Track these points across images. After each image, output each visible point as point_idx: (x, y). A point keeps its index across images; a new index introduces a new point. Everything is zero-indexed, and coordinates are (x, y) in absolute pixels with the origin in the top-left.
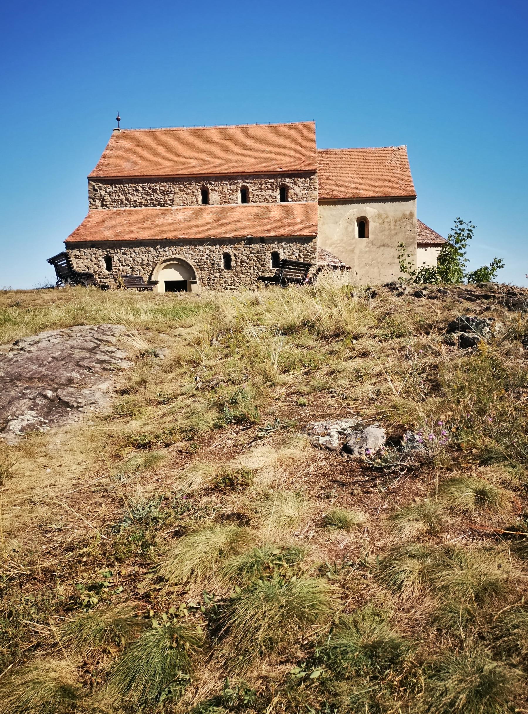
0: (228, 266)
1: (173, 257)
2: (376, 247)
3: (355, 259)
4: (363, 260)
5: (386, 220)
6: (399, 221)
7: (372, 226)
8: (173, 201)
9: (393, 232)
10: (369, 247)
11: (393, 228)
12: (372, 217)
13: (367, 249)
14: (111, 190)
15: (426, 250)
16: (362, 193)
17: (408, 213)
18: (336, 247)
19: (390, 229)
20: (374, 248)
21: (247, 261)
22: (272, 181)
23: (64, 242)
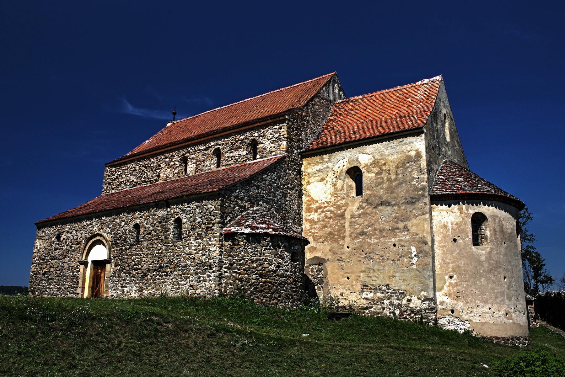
2: (372, 207)
4: (357, 227)
5: (384, 168)
6: (401, 167)
10: (363, 208)
11: (393, 177)
12: (366, 165)
13: (361, 211)
17: (413, 153)
18: (323, 212)
19: (389, 180)
22: (242, 137)
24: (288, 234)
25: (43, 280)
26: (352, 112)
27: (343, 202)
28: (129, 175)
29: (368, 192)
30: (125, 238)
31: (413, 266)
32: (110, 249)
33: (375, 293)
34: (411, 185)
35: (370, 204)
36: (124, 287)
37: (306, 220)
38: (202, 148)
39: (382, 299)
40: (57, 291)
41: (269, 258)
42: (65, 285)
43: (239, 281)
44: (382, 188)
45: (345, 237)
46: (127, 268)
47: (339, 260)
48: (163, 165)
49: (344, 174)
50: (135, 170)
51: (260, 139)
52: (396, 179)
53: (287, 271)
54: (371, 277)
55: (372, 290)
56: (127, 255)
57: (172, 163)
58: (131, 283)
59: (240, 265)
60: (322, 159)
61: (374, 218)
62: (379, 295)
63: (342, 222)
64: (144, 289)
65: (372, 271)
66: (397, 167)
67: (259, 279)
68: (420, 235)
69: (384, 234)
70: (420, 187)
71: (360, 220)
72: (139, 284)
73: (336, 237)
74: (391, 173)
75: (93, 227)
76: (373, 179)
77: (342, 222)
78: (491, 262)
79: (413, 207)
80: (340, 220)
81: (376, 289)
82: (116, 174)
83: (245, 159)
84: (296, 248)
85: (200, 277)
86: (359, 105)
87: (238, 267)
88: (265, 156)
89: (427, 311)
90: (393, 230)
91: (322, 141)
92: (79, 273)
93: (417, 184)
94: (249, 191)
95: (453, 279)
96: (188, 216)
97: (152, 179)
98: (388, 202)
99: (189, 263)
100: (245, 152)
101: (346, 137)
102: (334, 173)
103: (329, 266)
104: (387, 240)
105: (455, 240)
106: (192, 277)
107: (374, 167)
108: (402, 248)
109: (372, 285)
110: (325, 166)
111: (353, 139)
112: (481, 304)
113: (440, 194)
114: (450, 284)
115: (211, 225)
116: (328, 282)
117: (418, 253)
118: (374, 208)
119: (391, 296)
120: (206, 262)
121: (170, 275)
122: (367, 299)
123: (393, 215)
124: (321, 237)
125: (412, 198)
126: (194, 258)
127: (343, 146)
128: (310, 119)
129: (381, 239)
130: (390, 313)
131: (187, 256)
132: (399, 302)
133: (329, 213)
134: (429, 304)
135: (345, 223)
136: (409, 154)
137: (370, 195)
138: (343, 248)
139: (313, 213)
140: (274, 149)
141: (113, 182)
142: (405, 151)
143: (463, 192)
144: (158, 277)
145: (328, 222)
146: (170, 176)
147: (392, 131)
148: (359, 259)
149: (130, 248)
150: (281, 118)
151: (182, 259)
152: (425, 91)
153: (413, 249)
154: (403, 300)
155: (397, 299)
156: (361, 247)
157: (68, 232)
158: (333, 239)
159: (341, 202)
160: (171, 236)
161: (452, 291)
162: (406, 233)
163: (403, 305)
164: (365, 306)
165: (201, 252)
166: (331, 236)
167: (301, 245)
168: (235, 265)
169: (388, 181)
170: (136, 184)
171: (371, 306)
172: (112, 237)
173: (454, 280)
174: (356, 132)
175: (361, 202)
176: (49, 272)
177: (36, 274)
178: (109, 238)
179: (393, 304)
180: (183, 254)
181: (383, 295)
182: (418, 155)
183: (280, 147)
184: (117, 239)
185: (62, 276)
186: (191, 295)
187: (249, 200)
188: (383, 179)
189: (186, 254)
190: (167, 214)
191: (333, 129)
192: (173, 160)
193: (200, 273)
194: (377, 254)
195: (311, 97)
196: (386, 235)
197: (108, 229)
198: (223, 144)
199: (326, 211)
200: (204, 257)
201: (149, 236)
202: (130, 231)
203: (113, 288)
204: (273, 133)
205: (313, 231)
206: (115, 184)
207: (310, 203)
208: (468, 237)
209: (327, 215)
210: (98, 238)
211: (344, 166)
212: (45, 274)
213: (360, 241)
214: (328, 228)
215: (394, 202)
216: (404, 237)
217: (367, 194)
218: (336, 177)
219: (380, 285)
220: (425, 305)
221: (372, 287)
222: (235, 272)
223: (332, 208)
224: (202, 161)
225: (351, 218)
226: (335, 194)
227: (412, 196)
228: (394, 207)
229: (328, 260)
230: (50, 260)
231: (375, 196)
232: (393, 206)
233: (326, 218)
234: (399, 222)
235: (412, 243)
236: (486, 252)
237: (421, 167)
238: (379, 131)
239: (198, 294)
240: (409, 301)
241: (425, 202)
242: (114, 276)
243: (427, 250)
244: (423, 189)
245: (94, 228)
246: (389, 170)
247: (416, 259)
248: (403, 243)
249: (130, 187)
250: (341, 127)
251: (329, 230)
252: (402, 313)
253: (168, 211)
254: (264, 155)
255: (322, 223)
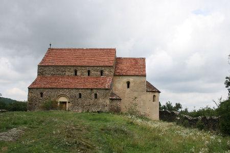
7: (131, 85)
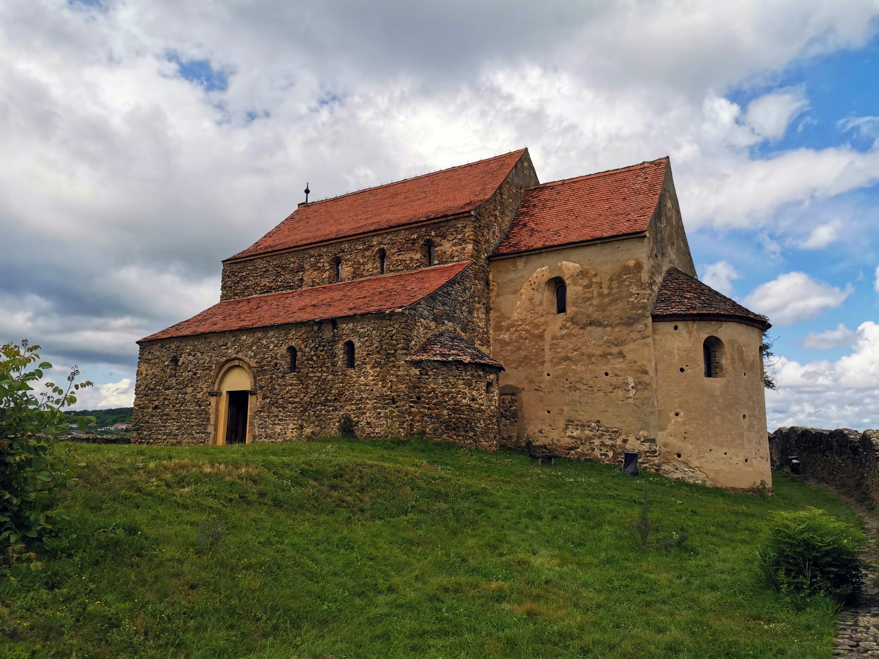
0: (293, 367)
1: (233, 356)
2: (579, 327)
3: (545, 350)
4: (559, 350)
6: (616, 280)
7: (571, 291)
8: (302, 280)
9: (607, 300)
10: (567, 328)
11: (606, 291)
12: (572, 276)
13: (565, 332)
14: (243, 274)
15: (676, 328)
16: (561, 240)
17: (631, 263)
18: (516, 331)
19: (601, 295)
20: (575, 331)
21: (315, 358)
23: (138, 343)
24: (483, 362)
25: (153, 416)
26: (549, 204)
27: (542, 320)
28: (259, 277)
29: (574, 309)
30: (276, 364)
31: (630, 400)
32: (255, 378)
33: (582, 431)
34: (628, 302)
35: (577, 323)
36: (276, 424)
37: (495, 340)
38: (361, 247)
39: (591, 438)
40: (177, 430)
41: (462, 390)
42: (188, 422)
43: (428, 418)
44: (591, 305)
45: (544, 362)
46: (280, 401)
47: (538, 390)
48: (307, 267)
49: (543, 285)
50: (268, 270)
51: (438, 240)
52: (609, 294)
53: (482, 405)
54: (576, 411)
55: (578, 427)
56: (279, 385)
57: (319, 265)
58: (286, 420)
59: (429, 398)
60: (515, 266)
61: (581, 341)
62: (587, 432)
63: (540, 344)
64: (305, 427)
65: (578, 404)
66: (611, 280)
67: (451, 415)
68: (639, 363)
69: (593, 360)
70: (639, 306)
71: (563, 343)
72: (297, 421)
73: (533, 362)
74: (603, 286)
75: (228, 348)
76: (580, 293)
77: (540, 344)
78: (727, 397)
79: (630, 329)
80: (537, 341)
81: (583, 426)
82: (240, 275)
83: (419, 264)
84: (492, 376)
85: (380, 413)
86: (557, 194)
87: (427, 401)
88: (446, 262)
89: (648, 454)
90: (604, 356)
91: (513, 242)
92: (209, 407)
93: (636, 301)
94: (434, 309)
95: (680, 416)
96: (362, 339)
97: (292, 284)
98: (600, 323)
99: (365, 396)
100: (418, 256)
101: (544, 239)
102: (531, 285)
103: (524, 396)
104: (597, 368)
105: (682, 370)
106: (370, 413)
107: (581, 279)
108: (616, 378)
109: (579, 420)
110: (519, 275)
111: (556, 243)
112: (714, 448)
113: (665, 314)
114: (676, 422)
115: (393, 351)
116: (523, 417)
117: (636, 385)
118: (581, 328)
119: (602, 434)
120: (387, 396)
121: (340, 410)
122: (573, 438)
123: (605, 338)
124: (514, 361)
125: (629, 318)
126: (372, 390)
127: (543, 251)
128: (498, 214)
129: (590, 366)
130: (601, 455)
131: (363, 388)
132: (612, 442)
133: (524, 332)
134: (650, 446)
135: (544, 346)
136: (626, 264)
137: (576, 313)
138: (542, 376)
139: (504, 332)
140: (457, 253)
141: (236, 285)
142: (621, 259)
143: (693, 312)
144: (323, 412)
145: (523, 343)
146: (318, 281)
147: (605, 235)
148: (563, 389)
149: (282, 377)
150: (467, 215)
151: (356, 392)
152: (647, 178)
153: (631, 381)
154: (618, 439)
155: (610, 439)
156: (565, 374)
157: (189, 354)
158: (530, 365)
159: (539, 319)
160: (339, 363)
161: (678, 430)
162: (621, 360)
163: (618, 447)
164: (570, 446)
165: (380, 383)
166: (528, 361)
167: (496, 373)
168: (423, 399)
169: (598, 296)
170: (270, 289)
171: (577, 446)
172: (256, 362)
173: (681, 418)
174: (557, 233)
175: (564, 320)
176: (163, 405)
177: (143, 408)
178: (253, 363)
179: (606, 446)
180: (356, 385)
181: (592, 433)
182: (639, 266)
183: (465, 251)
184: (264, 365)
185: (183, 410)
186: (368, 434)
187: (435, 320)
188: (593, 294)
189: (361, 385)
190: (334, 336)
191: (525, 225)
192: (322, 261)
193: (379, 408)
194: (584, 384)
195: (499, 184)
196: (596, 361)
197: (250, 353)
198: (389, 244)
199: (520, 330)
200: (386, 388)
201: (310, 362)
202: (282, 356)
203: (261, 426)
204: (455, 233)
205: (504, 354)
206: (238, 288)
207: (500, 320)
208: (698, 366)
209: (522, 335)
210: (237, 363)
211: (543, 276)
212: (156, 407)
213: (564, 368)
214: (523, 351)
215: (606, 322)
216: (618, 364)
217: (572, 311)
218: (534, 289)
219: (589, 422)
220: (646, 447)
221: (578, 423)
222: (423, 407)
223: (527, 327)
224: (362, 264)
225: (552, 340)
226: (532, 310)
227: (629, 315)
228: (607, 329)
229: (523, 389)
230: (163, 391)
231: (582, 314)
232: (605, 327)
233: (520, 339)
234: (613, 346)
235: (629, 372)
236: (721, 385)
237: (642, 280)
238: (587, 234)
239: (377, 433)
240: (625, 441)
241: (645, 324)
242: (261, 411)
243: (648, 381)
244: (644, 307)
245: (230, 351)
246: (601, 283)
247: (634, 391)
248: (617, 372)
249: (261, 293)
250: (536, 224)
251: (524, 353)
252: (616, 455)
253: (334, 333)
254: (444, 260)
255: (515, 344)
